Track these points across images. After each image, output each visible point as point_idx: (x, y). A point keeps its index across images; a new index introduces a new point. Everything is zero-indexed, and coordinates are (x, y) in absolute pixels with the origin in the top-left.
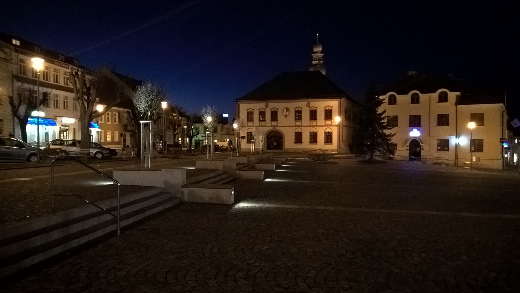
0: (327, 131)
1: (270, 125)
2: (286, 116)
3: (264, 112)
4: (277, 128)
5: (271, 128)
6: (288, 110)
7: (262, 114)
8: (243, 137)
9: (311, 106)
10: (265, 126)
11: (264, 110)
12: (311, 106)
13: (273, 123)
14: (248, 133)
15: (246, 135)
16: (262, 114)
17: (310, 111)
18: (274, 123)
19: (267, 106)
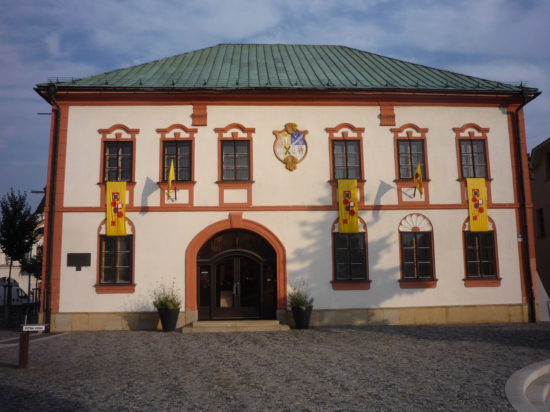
0: (475, 227)
1: (217, 204)
2: (290, 164)
4: (247, 215)
5: (224, 216)
6: (294, 132)
7: (177, 153)
8: (79, 261)
9: (399, 124)
10: (189, 207)
11: (184, 135)
12: (399, 124)
13: (227, 192)
14: (103, 239)
15: (91, 247)
16: (177, 153)
17: (398, 142)
18: (235, 196)
19: (200, 119)
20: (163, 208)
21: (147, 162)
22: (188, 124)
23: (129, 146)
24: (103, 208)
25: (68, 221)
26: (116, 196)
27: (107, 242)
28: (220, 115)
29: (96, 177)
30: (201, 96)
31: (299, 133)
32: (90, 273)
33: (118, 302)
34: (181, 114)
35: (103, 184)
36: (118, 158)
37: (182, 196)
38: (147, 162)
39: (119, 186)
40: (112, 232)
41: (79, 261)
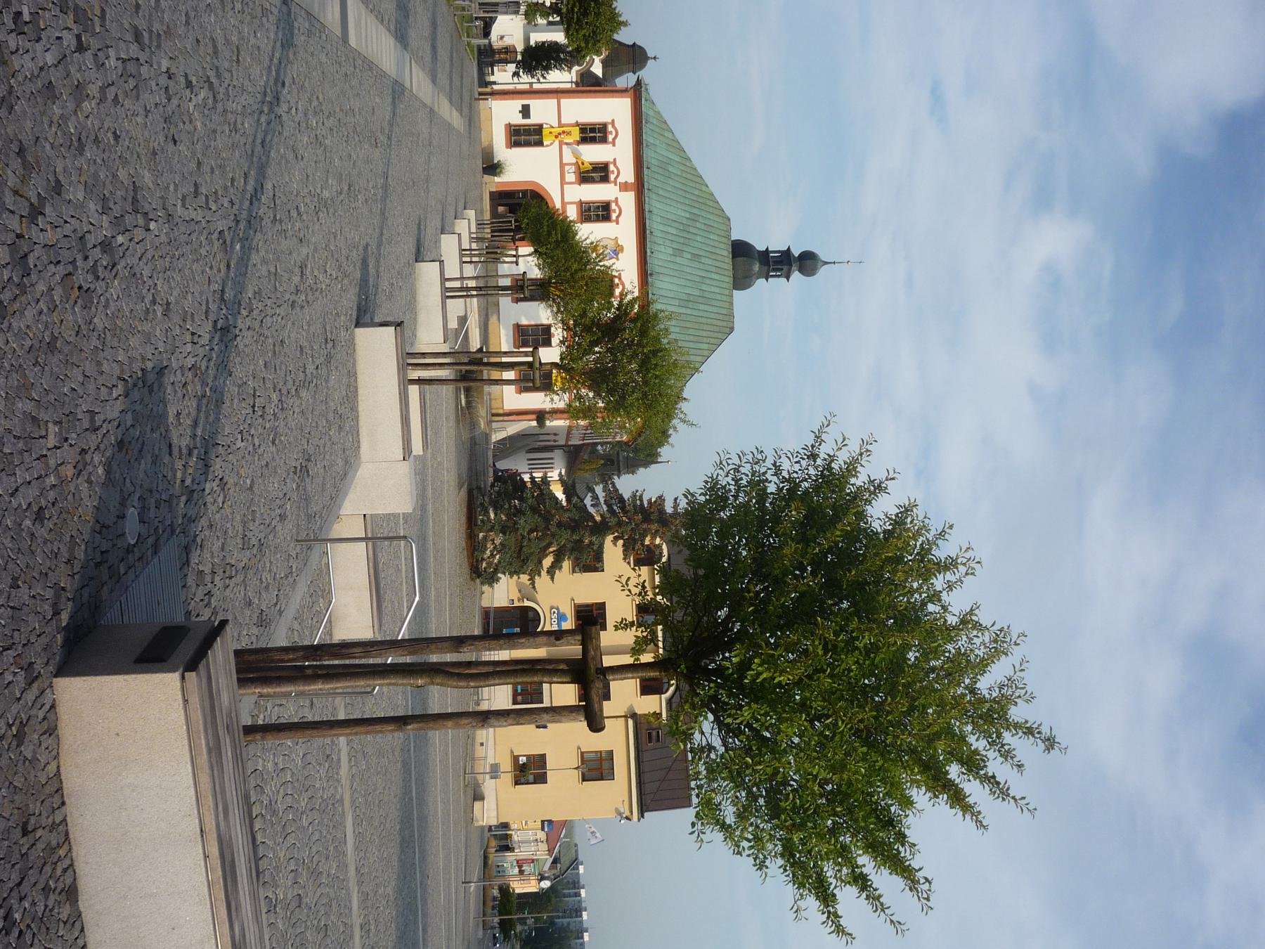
1: (566, 200)
3: (605, 179)
7: (600, 173)
8: (526, 111)
10: (563, 182)
11: (612, 177)
13: (574, 207)
14: (541, 126)
15: (534, 119)
16: (600, 173)
19: (624, 187)
20: (562, 165)
21: (593, 153)
22: (619, 180)
23: (604, 140)
24: (560, 125)
25: (551, 103)
26: (569, 133)
27: (538, 129)
28: (627, 201)
29: (583, 120)
30: (639, 187)
31: (617, 254)
32: (518, 120)
33: (499, 139)
34: (628, 175)
35: (577, 124)
36: (593, 133)
37: (571, 177)
38: (593, 153)
39: (576, 135)
40: (545, 132)
41: (526, 111)
